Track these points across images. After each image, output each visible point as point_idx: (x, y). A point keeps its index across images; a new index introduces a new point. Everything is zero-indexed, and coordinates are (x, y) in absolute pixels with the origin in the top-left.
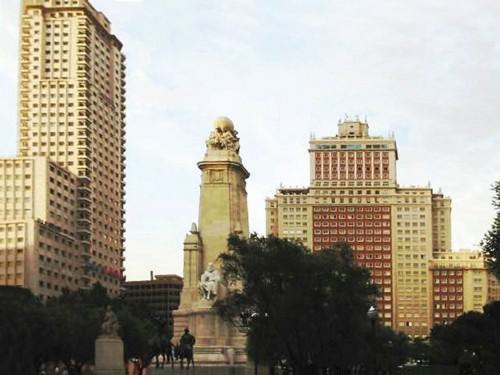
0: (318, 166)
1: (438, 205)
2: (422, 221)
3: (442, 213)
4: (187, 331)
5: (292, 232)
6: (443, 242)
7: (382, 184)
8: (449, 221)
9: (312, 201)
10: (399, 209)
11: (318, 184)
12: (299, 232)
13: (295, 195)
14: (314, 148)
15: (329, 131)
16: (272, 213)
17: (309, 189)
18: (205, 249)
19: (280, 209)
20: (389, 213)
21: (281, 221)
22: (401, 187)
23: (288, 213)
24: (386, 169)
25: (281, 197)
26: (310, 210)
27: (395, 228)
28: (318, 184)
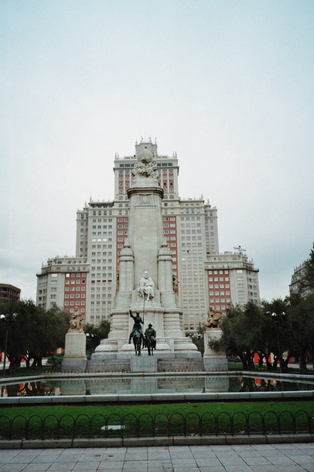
0: (121, 182)
1: (208, 214)
2: (199, 228)
3: (212, 222)
4: (150, 326)
5: (99, 240)
6: (213, 246)
7: (169, 197)
8: (217, 228)
9: (116, 213)
10: (182, 219)
11: (121, 198)
12: (105, 240)
13: (102, 207)
14: (118, 166)
15: (128, 151)
16: (82, 224)
17: (114, 202)
18: (136, 261)
19: (90, 220)
20: (175, 222)
21: (91, 230)
22: (182, 200)
23: (97, 224)
24: (171, 184)
25: (91, 210)
26: (115, 220)
27: (179, 235)
28: (121, 198)
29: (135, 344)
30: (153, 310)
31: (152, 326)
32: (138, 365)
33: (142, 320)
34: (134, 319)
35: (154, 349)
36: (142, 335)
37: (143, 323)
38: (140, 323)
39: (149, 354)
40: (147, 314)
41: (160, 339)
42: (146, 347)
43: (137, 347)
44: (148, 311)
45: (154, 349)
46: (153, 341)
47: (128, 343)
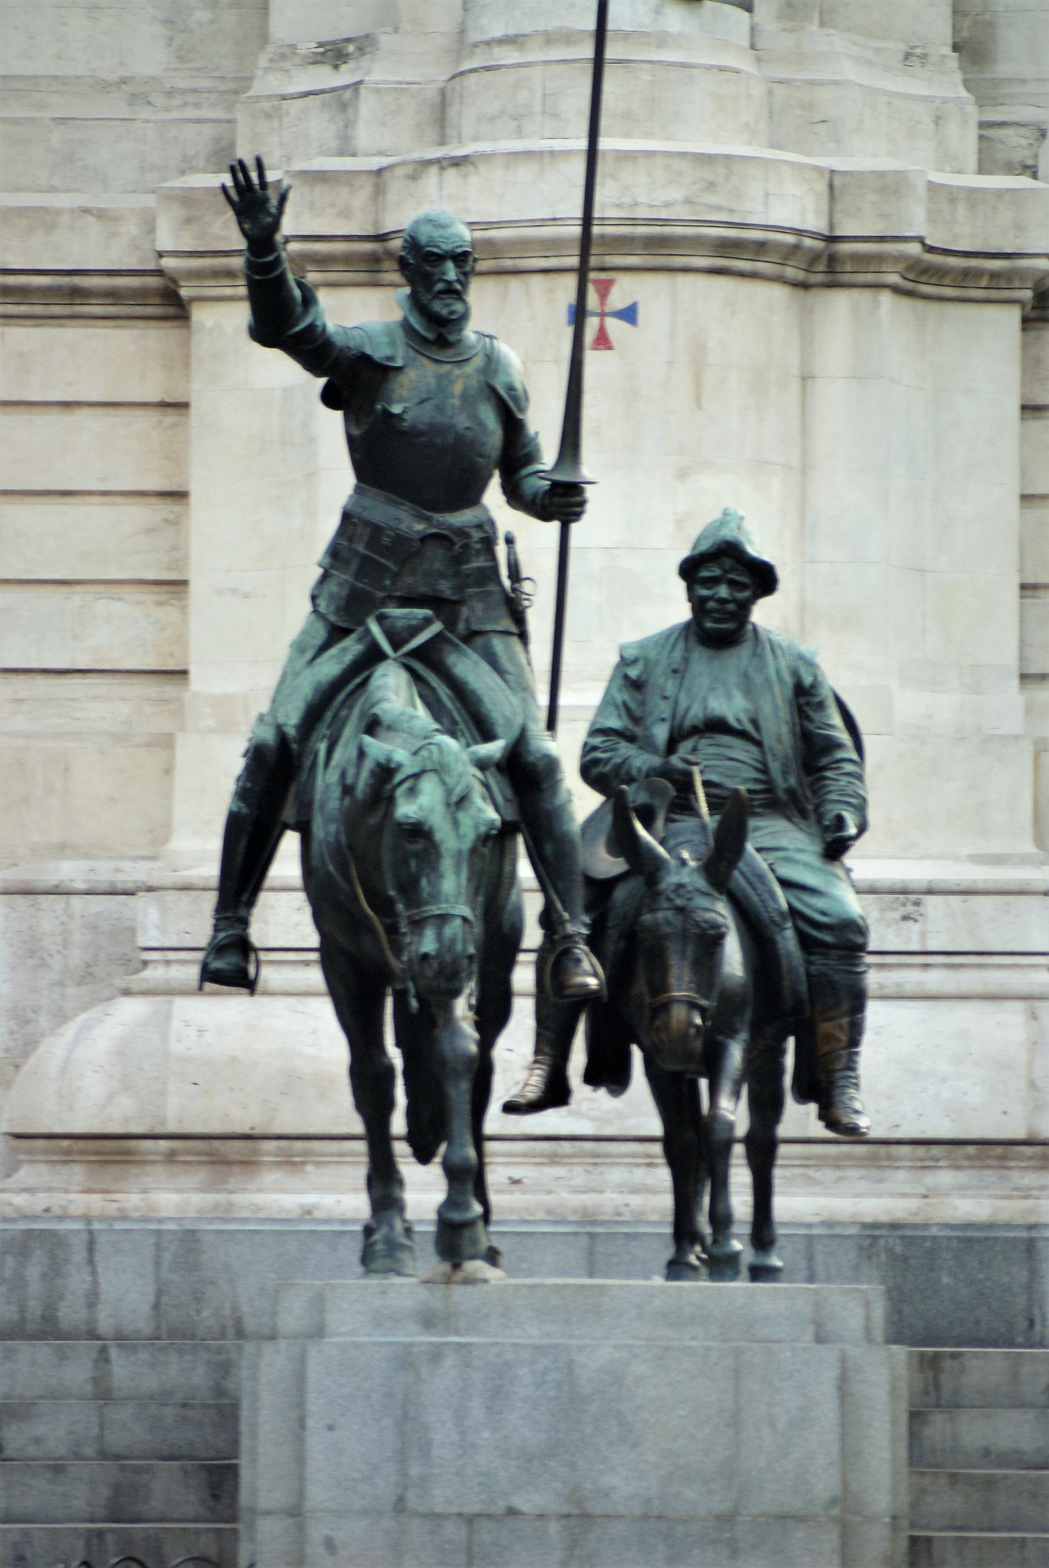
29: (356, 983)
30: (789, 207)
31: (763, 579)
32: (439, 1499)
33: (544, 424)
34: (330, 398)
35: (799, 1118)
36: (524, 776)
37: (562, 503)
38: (493, 497)
39: (693, 1240)
40: (629, 315)
41: (930, 901)
42: (608, 1073)
43: (395, 1055)
44: (661, 250)
45: (799, 1118)
46: (788, 940)
47: (193, 972)
